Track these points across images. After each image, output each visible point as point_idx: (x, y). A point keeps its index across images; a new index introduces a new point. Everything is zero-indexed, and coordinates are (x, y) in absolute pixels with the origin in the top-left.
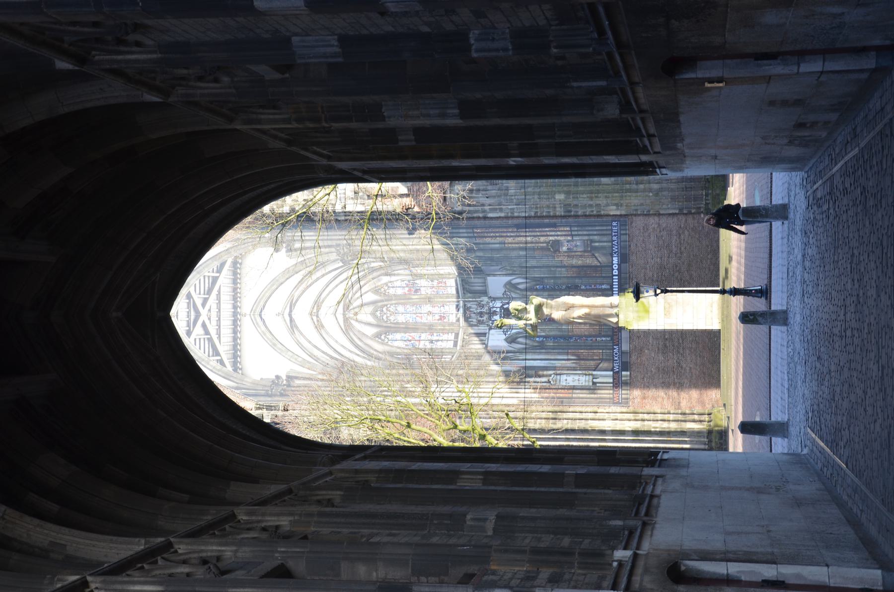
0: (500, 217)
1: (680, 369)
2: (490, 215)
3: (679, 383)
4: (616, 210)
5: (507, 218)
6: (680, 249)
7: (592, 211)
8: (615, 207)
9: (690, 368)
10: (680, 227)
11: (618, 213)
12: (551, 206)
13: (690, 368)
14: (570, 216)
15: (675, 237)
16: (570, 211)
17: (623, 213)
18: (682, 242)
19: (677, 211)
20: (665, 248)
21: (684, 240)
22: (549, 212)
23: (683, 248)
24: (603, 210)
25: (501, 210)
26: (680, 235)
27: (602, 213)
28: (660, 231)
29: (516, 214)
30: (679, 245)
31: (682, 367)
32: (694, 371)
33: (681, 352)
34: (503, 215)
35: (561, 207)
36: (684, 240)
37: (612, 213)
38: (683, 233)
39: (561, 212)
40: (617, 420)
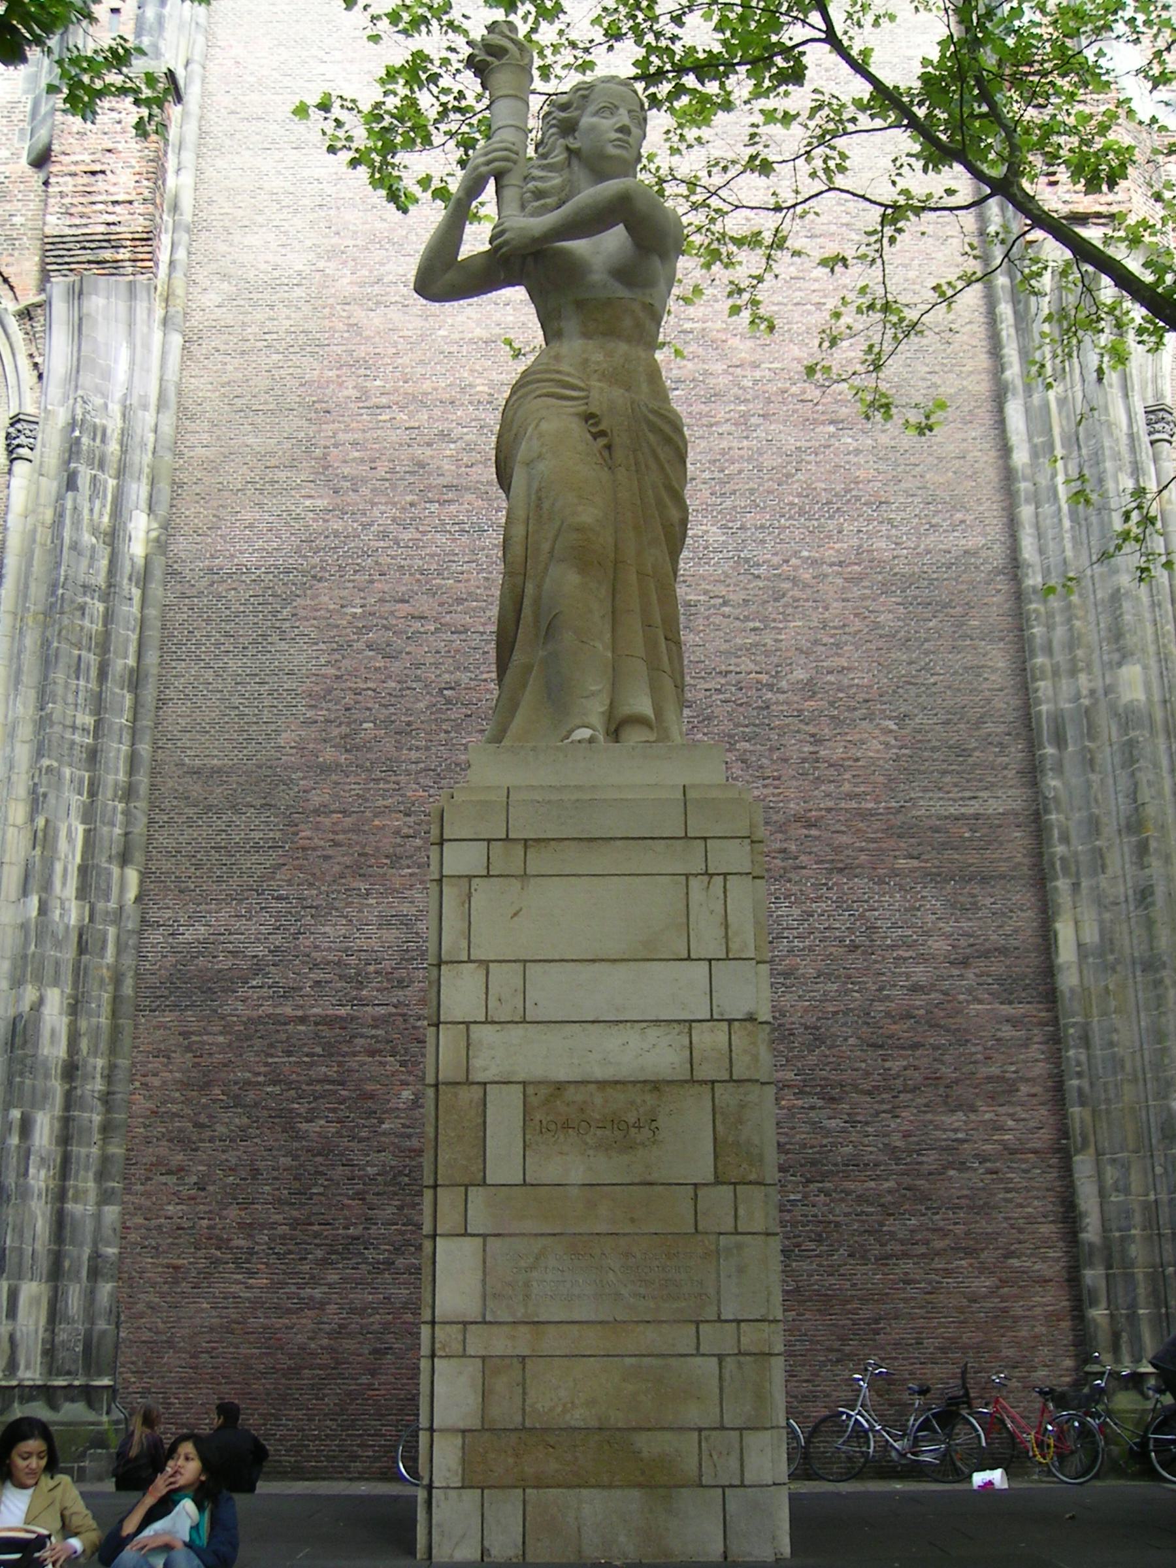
0: (1006, 450)
1: (319, 1253)
2: (1015, 411)
3: (251, 1252)
4: (1080, 945)
5: (1008, 476)
6: (906, 1255)
7: (1065, 839)
8: (1091, 935)
9: (322, 1306)
10: (1010, 1255)
11: (1066, 953)
12: (1080, 653)
13: (322, 1306)
14: (1032, 745)
15: (959, 1229)
16: (1060, 740)
17: (1068, 980)
18: (938, 1264)
19: (1091, 1233)
20: (907, 1180)
21: (948, 1273)
22: (1049, 650)
23: (907, 1266)
24: (1076, 886)
25: (1042, 451)
26: (970, 1252)
27: (1062, 884)
28: (983, 1159)
29: (1026, 512)
30: (922, 1249)
31: (324, 1263)
32: (306, 1321)
33: (400, 1262)
34: (1021, 457)
35: (1078, 696)
36: (948, 1273)
37: (1064, 931)
38: (983, 1270)
39: (1055, 699)
40: (82, 949)
